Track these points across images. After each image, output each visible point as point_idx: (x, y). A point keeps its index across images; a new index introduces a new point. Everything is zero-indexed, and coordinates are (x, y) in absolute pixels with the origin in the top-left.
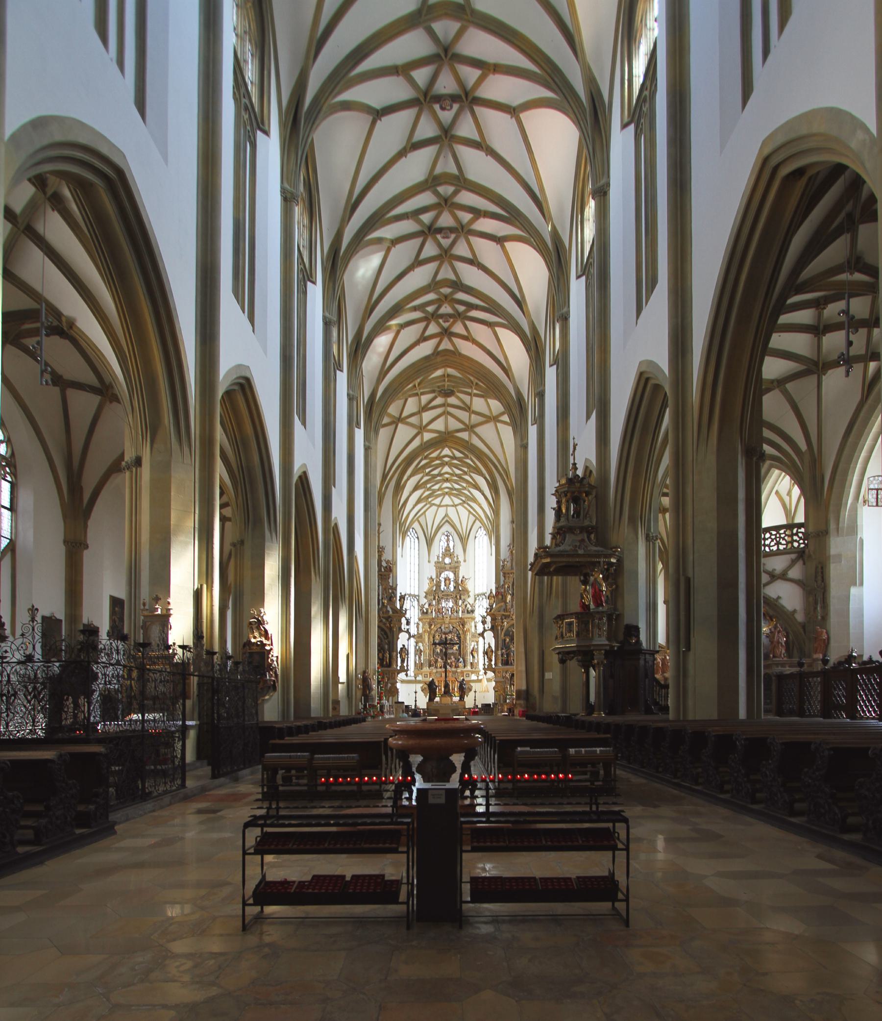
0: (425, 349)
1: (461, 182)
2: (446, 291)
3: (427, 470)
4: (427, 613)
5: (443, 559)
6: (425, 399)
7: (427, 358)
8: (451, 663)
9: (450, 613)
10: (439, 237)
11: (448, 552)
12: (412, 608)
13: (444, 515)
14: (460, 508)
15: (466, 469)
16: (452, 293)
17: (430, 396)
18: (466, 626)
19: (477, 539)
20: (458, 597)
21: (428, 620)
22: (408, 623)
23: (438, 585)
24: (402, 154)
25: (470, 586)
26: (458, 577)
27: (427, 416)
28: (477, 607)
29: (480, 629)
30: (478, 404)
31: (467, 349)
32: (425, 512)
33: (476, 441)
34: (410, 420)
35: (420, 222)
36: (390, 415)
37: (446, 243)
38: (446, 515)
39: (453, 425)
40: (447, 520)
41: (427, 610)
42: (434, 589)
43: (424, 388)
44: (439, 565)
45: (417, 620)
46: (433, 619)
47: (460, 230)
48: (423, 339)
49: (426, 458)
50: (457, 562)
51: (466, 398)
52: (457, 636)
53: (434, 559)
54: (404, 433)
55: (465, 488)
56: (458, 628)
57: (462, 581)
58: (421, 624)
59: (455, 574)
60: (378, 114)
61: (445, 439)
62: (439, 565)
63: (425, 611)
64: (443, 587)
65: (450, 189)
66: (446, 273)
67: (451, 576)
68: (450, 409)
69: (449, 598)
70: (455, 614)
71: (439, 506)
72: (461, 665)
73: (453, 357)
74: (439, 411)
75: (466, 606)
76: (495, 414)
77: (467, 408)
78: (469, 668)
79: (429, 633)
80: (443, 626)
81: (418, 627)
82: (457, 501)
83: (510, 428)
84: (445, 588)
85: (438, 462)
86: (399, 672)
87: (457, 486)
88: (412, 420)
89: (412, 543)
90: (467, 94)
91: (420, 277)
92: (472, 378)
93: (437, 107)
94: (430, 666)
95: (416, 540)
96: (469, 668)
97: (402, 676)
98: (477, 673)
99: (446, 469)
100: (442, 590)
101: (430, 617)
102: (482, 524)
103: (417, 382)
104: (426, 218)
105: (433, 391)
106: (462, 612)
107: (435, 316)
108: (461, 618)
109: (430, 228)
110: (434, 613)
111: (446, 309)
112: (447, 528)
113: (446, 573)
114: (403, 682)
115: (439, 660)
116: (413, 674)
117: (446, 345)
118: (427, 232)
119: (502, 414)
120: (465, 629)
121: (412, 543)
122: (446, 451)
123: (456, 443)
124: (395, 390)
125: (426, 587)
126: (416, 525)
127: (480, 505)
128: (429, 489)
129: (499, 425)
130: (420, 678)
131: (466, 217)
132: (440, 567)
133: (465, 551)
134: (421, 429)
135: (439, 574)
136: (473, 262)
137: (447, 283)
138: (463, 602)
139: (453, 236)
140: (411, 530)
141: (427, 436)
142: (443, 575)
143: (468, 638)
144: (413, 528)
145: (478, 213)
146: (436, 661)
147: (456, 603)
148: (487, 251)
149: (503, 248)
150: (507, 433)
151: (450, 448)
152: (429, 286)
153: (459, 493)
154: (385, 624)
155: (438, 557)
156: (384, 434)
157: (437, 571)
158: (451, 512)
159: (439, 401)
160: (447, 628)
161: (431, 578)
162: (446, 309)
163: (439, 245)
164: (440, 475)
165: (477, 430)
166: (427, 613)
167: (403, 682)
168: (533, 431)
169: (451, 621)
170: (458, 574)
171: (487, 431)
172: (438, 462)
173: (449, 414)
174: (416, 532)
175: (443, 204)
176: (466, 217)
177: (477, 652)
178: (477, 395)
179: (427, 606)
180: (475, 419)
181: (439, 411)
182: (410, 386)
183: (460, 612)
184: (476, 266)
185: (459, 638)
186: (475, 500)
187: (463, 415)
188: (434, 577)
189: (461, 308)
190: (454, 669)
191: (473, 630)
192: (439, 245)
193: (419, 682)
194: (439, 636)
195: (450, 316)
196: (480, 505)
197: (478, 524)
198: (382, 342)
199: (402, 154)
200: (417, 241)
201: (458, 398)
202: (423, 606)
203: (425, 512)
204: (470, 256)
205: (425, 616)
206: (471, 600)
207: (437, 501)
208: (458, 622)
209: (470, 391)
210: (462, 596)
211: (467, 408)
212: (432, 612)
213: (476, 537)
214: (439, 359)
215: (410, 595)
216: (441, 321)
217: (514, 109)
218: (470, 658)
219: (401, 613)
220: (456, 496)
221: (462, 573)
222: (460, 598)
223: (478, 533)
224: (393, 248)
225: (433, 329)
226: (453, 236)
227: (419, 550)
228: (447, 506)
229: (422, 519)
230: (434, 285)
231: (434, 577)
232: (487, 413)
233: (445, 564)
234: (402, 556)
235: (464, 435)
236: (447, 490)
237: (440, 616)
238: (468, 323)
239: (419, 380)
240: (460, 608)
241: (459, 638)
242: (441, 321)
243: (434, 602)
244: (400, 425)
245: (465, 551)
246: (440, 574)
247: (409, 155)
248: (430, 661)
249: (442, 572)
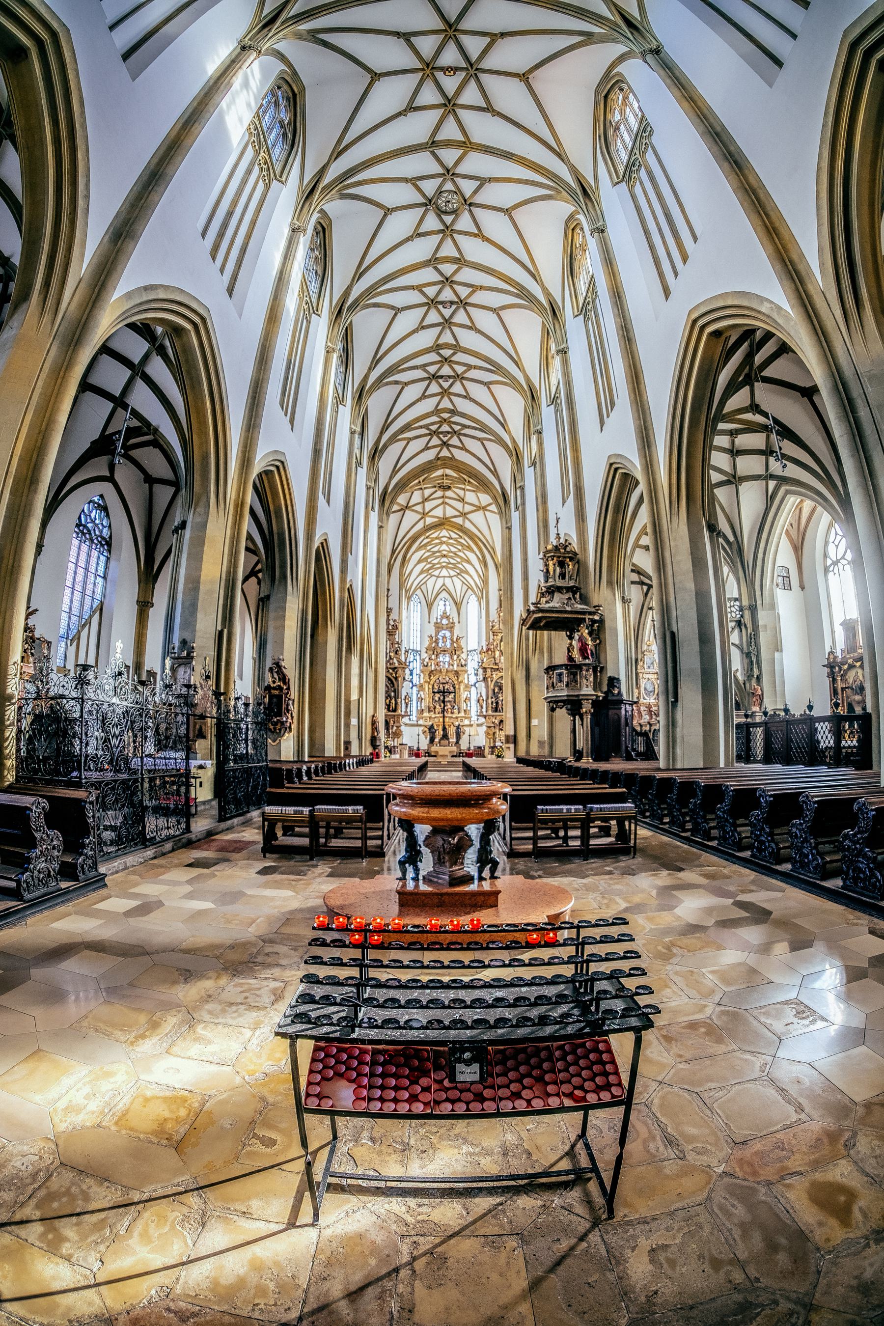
0: (430, 455)
1: (457, 348)
2: (446, 415)
3: (429, 548)
6: (427, 492)
7: (430, 462)
10: (440, 381)
14: (455, 579)
15: (460, 548)
16: (450, 417)
17: (434, 490)
22: (411, 674)
23: (437, 642)
25: (462, 643)
27: (429, 505)
28: (469, 661)
29: (473, 679)
30: (470, 497)
31: (459, 455)
32: (425, 582)
33: (468, 525)
34: (414, 508)
36: (399, 504)
37: (446, 385)
38: (444, 585)
39: (450, 512)
40: (444, 588)
43: (427, 484)
45: (418, 672)
48: (427, 448)
49: (427, 537)
51: (461, 493)
53: (433, 620)
54: (410, 517)
55: (459, 563)
58: (422, 675)
60: (397, 311)
61: (442, 523)
64: (441, 644)
65: (451, 352)
66: (446, 404)
67: (448, 634)
68: (447, 500)
71: (438, 577)
72: (456, 711)
73: (451, 463)
74: (440, 501)
76: (483, 504)
77: (462, 500)
78: (462, 714)
82: (452, 573)
83: (498, 516)
85: (437, 541)
86: (403, 716)
87: (452, 561)
88: (419, 508)
90: (461, 301)
91: (428, 405)
92: (465, 477)
93: (440, 307)
94: (430, 711)
96: (462, 714)
97: (406, 720)
98: (470, 718)
99: (444, 547)
101: (430, 669)
103: (421, 479)
105: (435, 487)
107: (436, 433)
109: (433, 376)
111: (445, 428)
112: (444, 595)
113: (443, 632)
114: (406, 725)
115: (438, 706)
116: (415, 719)
117: (445, 453)
119: (490, 504)
122: (444, 533)
123: (452, 526)
124: (402, 486)
125: (427, 643)
126: (419, 592)
127: (471, 577)
128: (430, 563)
129: (486, 513)
130: (421, 722)
132: (438, 627)
134: (424, 515)
136: (467, 397)
137: (445, 410)
139: (451, 380)
141: (429, 521)
145: (470, 367)
146: (435, 708)
147: (452, 657)
148: (478, 392)
149: (489, 388)
150: (495, 520)
151: (447, 530)
152: (433, 412)
153: (455, 567)
154: (391, 674)
156: (394, 518)
158: (448, 582)
159: (439, 493)
162: (445, 428)
163: (441, 387)
164: (439, 551)
165: (468, 516)
167: (406, 725)
168: (515, 516)
171: (477, 518)
172: (437, 541)
173: (446, 503)
176: (460, 369)
177: (470, 701)
178: (468, 490)
179: (427, 660)
180: (468, 508)
181: (440, 501)
182: (417, 481)
185: (454, 688)
186: (467, 572)
187: (459, 505)
188: (433, 635)
189: (457, 428)
190: (450, 715)
191: (466, 682)
192: (441, 387)
193: (421, 725)
195: (448, 433)
196: (471, 577)
197: (470, 591)
198: (394, 451)
201: (454, 492)
202: (424, 660)
203: (425, 582)
206: (464, 656)
207: (436, 573)
209: (463, 486)
211: (462, 500)
214: (439, 462)
215: (413, 650)
216: (441, 436)
218: (463, 706)
219: (404, 665)
220: (452, 569)
221: (457, 632)
225: (435, 441)
226: (451, 380)
228: (444, 577)
229: (423, 587)
230: (437, 411)
231: (433, 635)
232: (477, 504)
235: (459, 521)
236: (444, 564)
238: (461, 437)
239: (423, 477)
241: (454, 688)
242: (441, 436)
244: (407, 511)
245: (459, 614)
248: (429, 708)
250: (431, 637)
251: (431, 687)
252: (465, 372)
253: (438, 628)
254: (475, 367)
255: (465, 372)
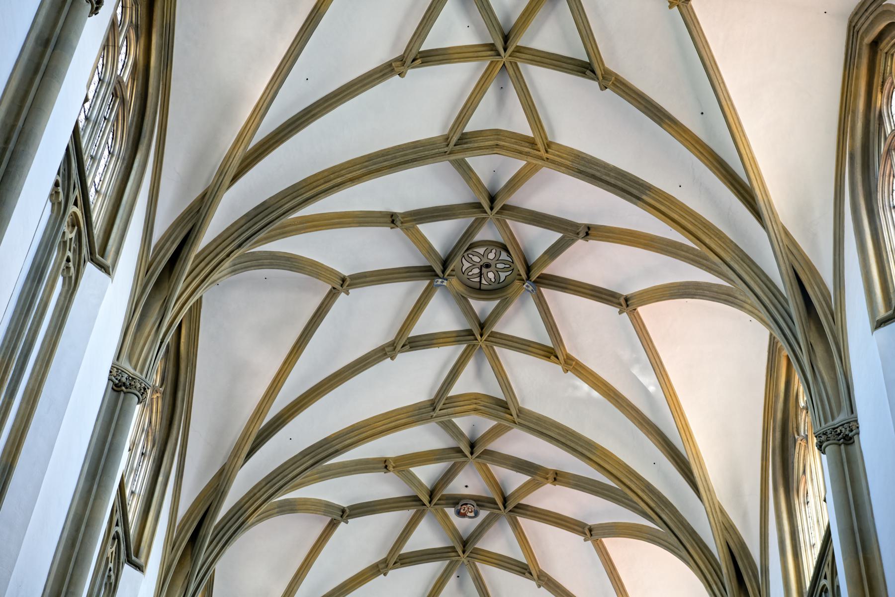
24: (378, 569)
35: (412, 480)
37: (465, 525)
47: (501, 506)
104: (426, 474)
118: (426, 502)
131: (515, 480)
139: (483, 514)
175: (467, 451)
176: (515, 480)
184: (534, 580)
199: (378, 569)
200: (403, 516)
204: (521, 557)
217: (627, 300)
224: (342, 524)
247: (391, 573)
252: (526, 489)
254: (558, 477)
255: (526, 489)
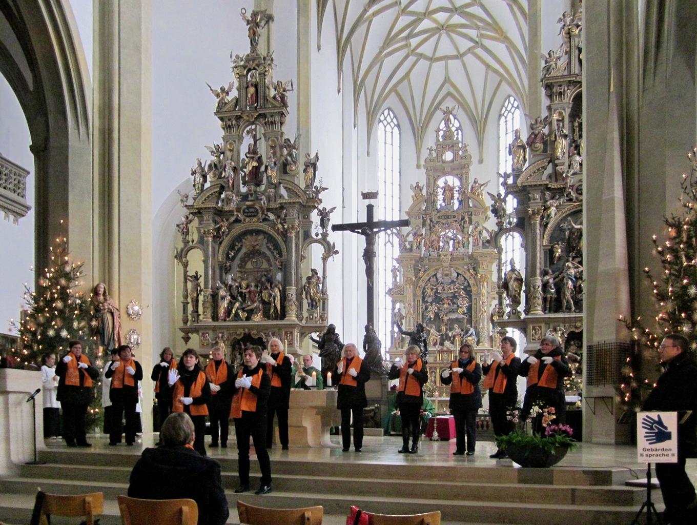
4: (411, 250)
5: (440, 154)
8: (454, 337)
9: (451, 249)
11: (449, 141)
12: (389, 245)
13: (441, 80)
18: (480, 270)
19: (503, 119)
20: (467, 219)
21: (413, 262)
23: (431, 200)
26: (467, 183)
38: (447, 80)
41: (411, 243)
42: (424, 208)
44: (432, 164)
46: (421, 258)
50: (467, 157)
52: (464, 289)
56: (467, 276)
57: (472, 188)
59: (460, 179)
62: (432, 164)
63: (408, 246)
64: (440, 202)
67: (453, 181)
69: (449, 221)
70: (461, 250)
75: (480, 233)
79: (416, 285)
80: (440, 271)
81: (395, 277)
84: (443, 204)
89: (389, 135)
95: (396, 129)
100: (439, 207)
101: (415, 253)
102: (513, 89)
106: (474, 246)
108: (471, 257)
110: (423, 249)
112: (449, 103)
120: (479, 276)
121: (389, 135)
126: (393, 100)
132: (435, 169)
133: (480, 143)
135: (432, 181)
138: (476, 228)
140: (386, 112)
142: (441, 182)
143: (484, 291)
144: (389, 109)
155: (431, 150)
157: (428, 175)
160: (446, 275)
161: (418, 186)
166: (411, 250)
169: (454, 263)
170: (467, 178)
174: (395, 117)
179: (411, 238)
183: (471, 246)
194: (432, 289)
197: (505, 88)
205: (410, 254)
208: (467, 264)
210: (473, 217)
212: (419, 247)
213: (500, 116)
222: (470, 223)
223: (504, 109)
227: (400, 147)
231: (423, 183)
233: (444, 162)
234: (368, 154)
237: (434, 254)
240: (471, 239)
243: (424, 231)
245: (480, 143)
246: (435, 181)
249: (439, 177)
250: (418, 188)
251: (419, 293)
253: (436, 170)
